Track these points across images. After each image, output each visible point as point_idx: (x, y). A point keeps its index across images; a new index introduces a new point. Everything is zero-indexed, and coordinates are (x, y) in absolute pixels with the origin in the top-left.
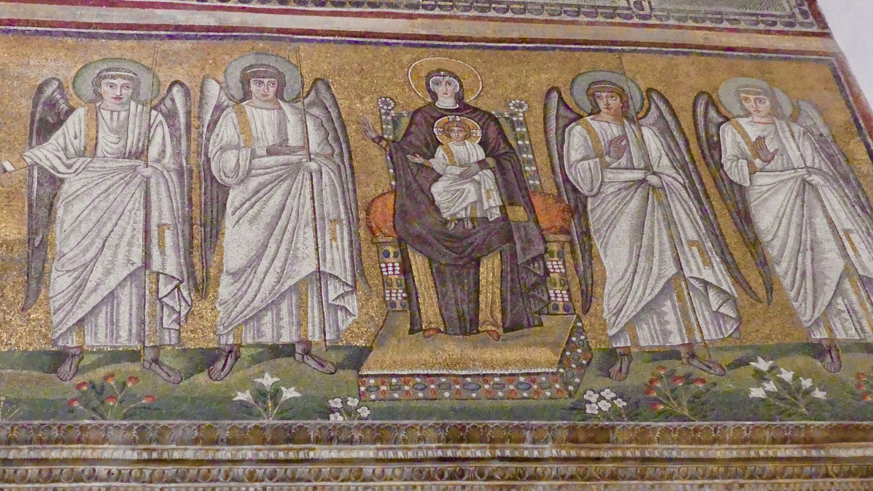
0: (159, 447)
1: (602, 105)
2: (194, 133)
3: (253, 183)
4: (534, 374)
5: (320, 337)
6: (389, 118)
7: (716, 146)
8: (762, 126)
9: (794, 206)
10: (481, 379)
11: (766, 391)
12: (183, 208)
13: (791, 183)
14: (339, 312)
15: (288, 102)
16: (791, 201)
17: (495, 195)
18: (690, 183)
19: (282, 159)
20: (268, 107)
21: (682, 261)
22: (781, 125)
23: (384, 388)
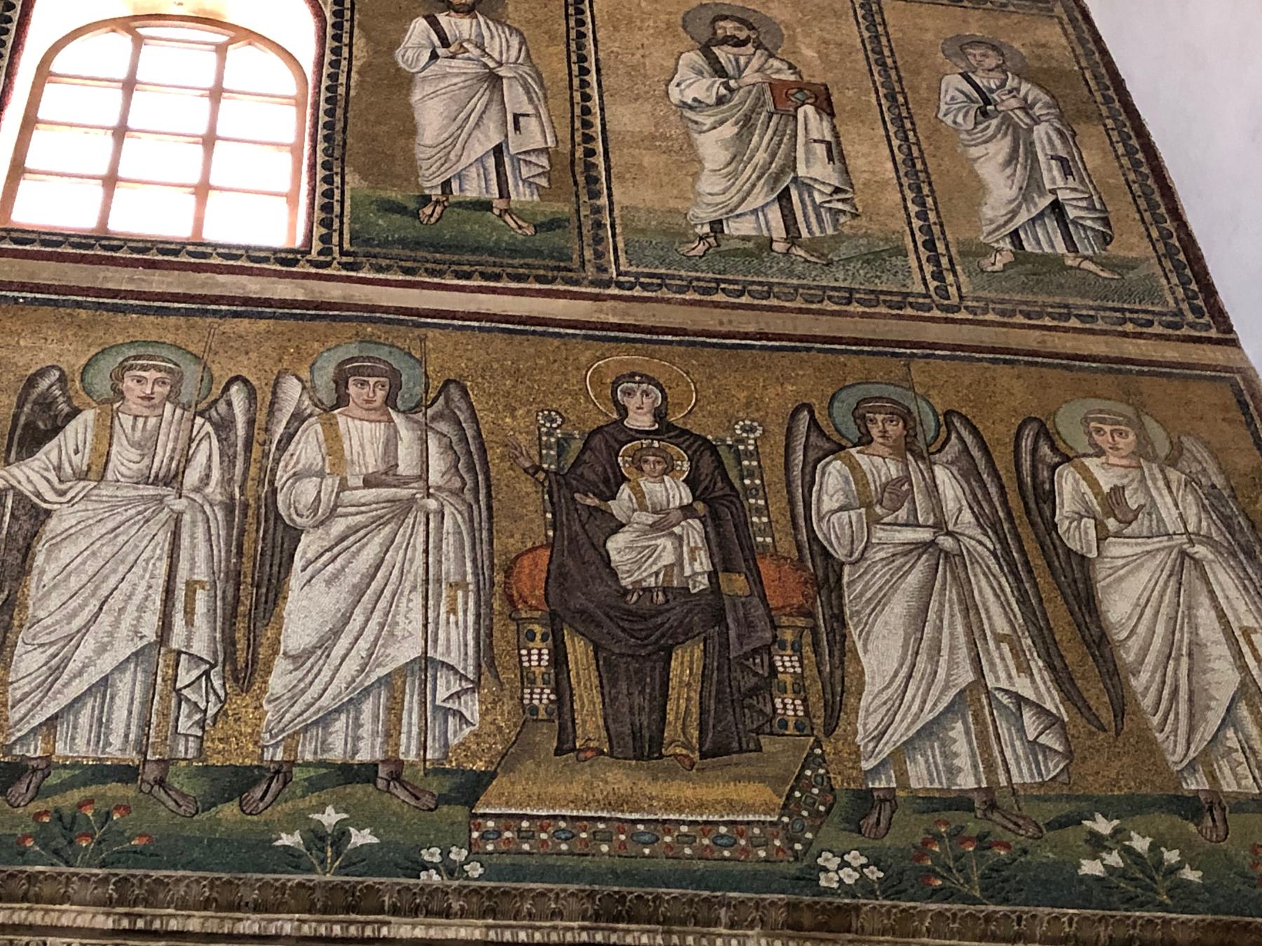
0: (149, 911)
1: (875, 432)
2: (256, 452)
3: (339, 526)
4: (741, 823)
5: (418, 755)
6: (553, 440)
10: (660, 827)
12: (228, 560)
14: (450, 719)
15: (404, 412)
16: (1161, 582)
17: (703, 556)
18: (1003, 549)
20: (373, 417)
22: (1150, 469)
23: (508, 834)
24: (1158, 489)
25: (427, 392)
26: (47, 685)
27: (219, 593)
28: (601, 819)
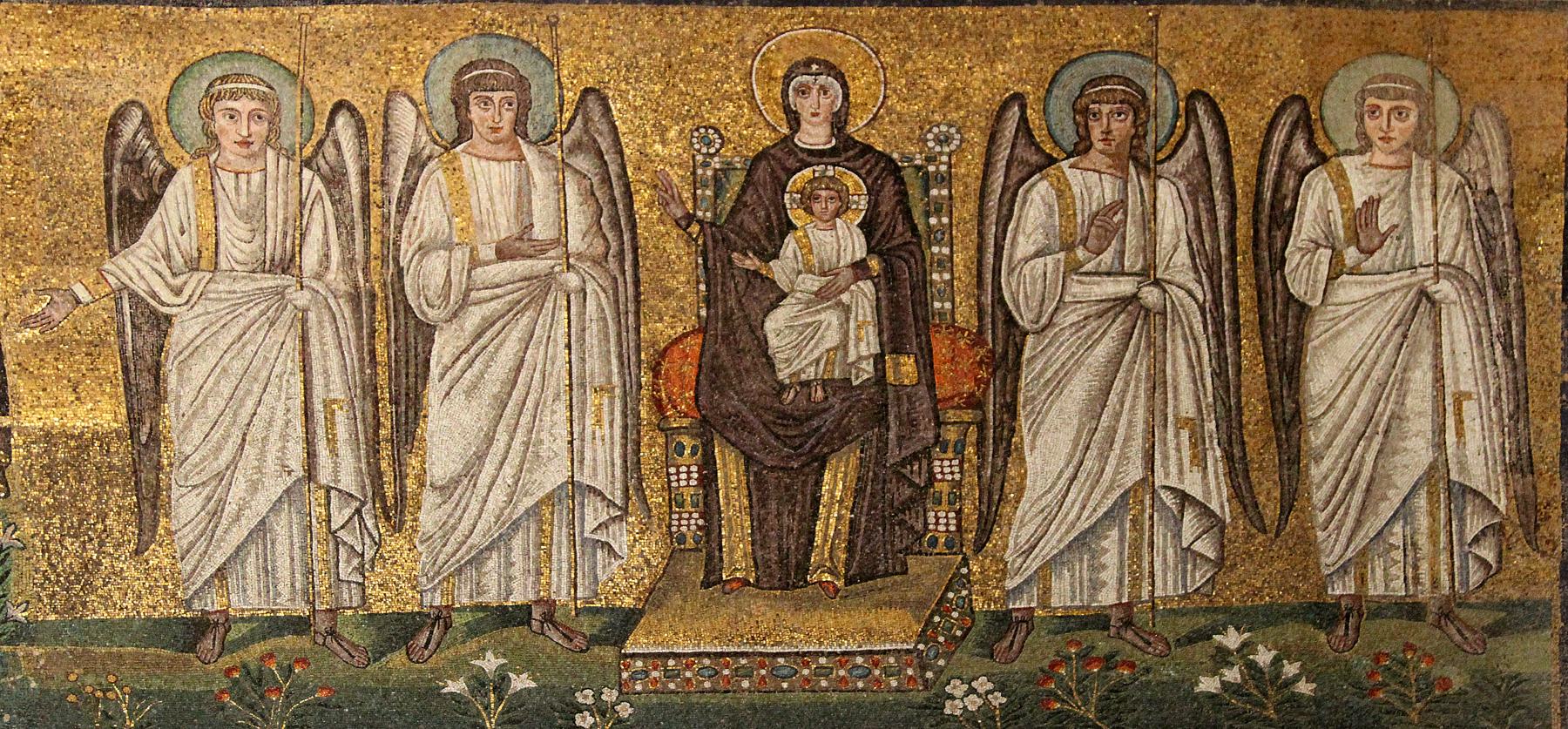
1: (1096, 134)
3: (473, 318)
4: (878, 652)
6: (709, 173)
7: (1282, 218)
8: (1381, 174)
9: (1384, 347)
11: (1222, 683)
12: (362, 371)
13: (1398, 295)
14: (599, 552)
16: (1383, 337)
17: (871, 335)
18: (1214, 301)
19: (520, 267)
20: (501, 155)
21: (1157, 456)
23: (655, 674)
24: (1420, 199)
25: (561, 111)
26: (209, 533)
27: (358, 414)
28: (743, 654)
